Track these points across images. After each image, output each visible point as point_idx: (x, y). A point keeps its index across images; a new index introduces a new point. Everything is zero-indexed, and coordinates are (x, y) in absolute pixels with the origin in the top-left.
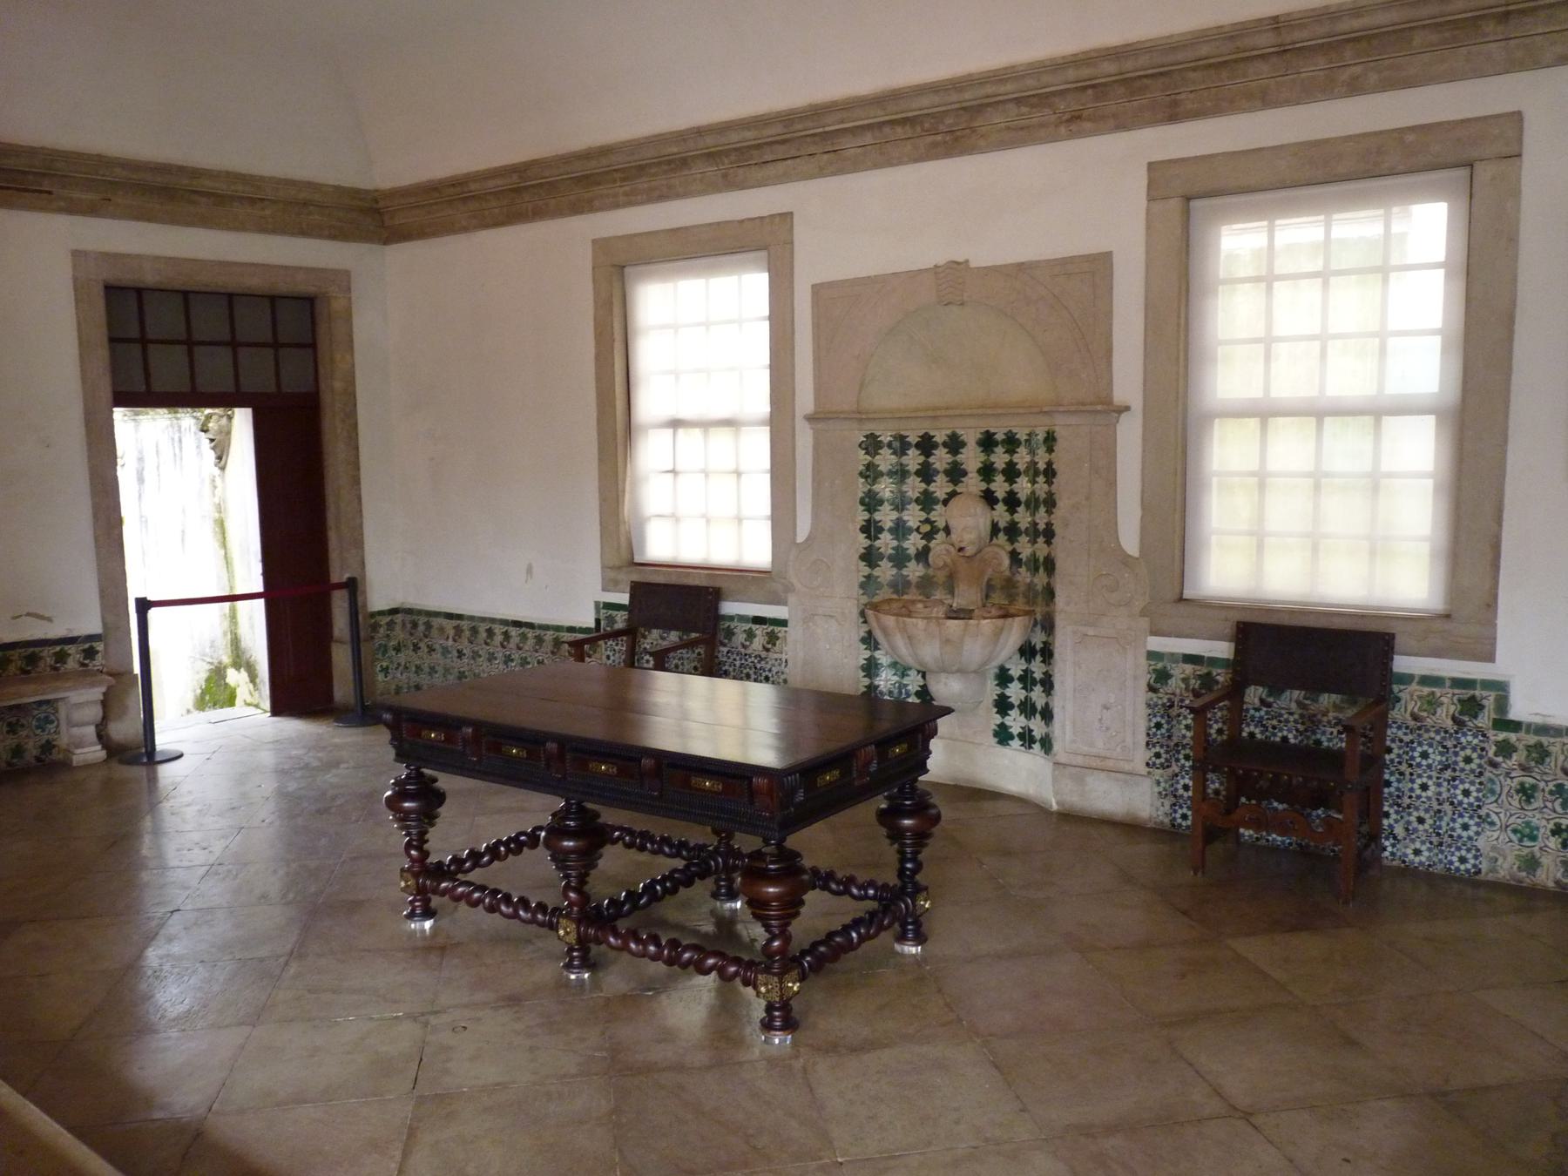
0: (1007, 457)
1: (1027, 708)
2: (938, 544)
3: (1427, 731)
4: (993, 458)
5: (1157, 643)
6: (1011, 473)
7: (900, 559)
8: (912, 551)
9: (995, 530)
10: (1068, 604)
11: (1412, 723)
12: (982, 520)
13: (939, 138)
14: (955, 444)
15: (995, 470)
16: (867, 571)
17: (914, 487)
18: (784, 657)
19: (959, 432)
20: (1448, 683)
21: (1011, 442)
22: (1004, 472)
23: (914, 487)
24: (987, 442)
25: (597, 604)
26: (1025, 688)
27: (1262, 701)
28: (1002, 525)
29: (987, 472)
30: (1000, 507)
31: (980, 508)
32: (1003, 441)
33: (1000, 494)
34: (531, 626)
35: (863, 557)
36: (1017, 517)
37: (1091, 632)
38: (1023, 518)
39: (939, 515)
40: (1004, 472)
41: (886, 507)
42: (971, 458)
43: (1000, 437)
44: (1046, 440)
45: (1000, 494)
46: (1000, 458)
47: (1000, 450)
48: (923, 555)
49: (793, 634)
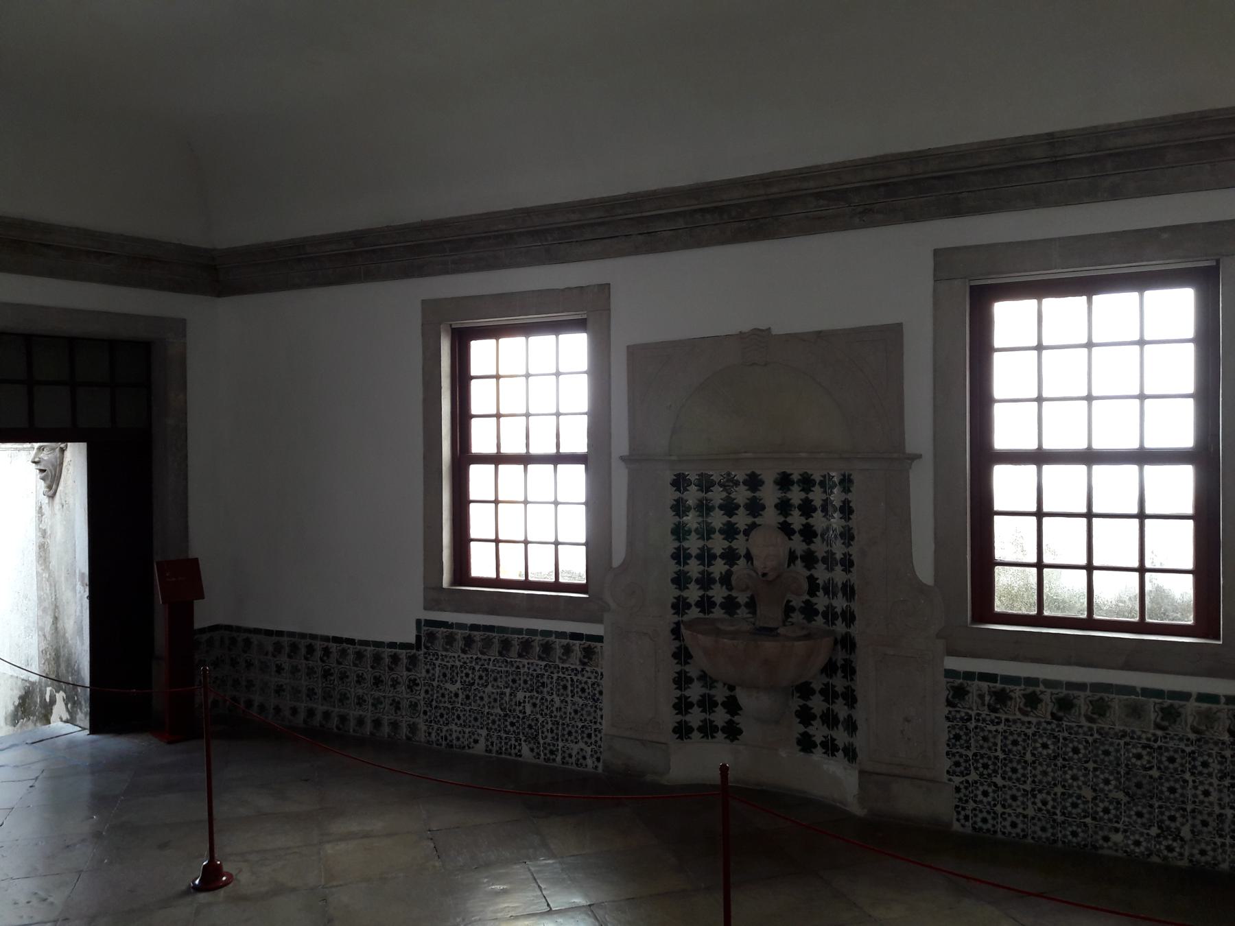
1: (830, 720)
3: (1207, 742)
4: (789, 495)
5: (952, 663)
6: (807, 508)
7: (706, 582)
8: (717, 576)
9: (792, 557)
11: (1193, 736)
13: (744, 224)
14: (754, 482)
16: (677, 593)
17: (718, 519)
18: (599, 670)
19: (758, 472)
20: (1223, 700)
21: (807, 483)
23: (718, 519)
24: (784, 481)
25: (418, 622)
26: (826, 700)
27: (1053, 715)
28: (799, 553)
29: (784, 507)
31: (780, 537)
32: (799, 481)
34: (351, 641)
35: (674, 581)
38: (819, 548)
39: (740, 544)
40: (800, 507)
41: (693, 536)
42: (769, 495)
43: (795, 477)
44: (842, 482)
46: (796, 496)
47: (796, 488)
48: (726, 580)
49: (606, 648)
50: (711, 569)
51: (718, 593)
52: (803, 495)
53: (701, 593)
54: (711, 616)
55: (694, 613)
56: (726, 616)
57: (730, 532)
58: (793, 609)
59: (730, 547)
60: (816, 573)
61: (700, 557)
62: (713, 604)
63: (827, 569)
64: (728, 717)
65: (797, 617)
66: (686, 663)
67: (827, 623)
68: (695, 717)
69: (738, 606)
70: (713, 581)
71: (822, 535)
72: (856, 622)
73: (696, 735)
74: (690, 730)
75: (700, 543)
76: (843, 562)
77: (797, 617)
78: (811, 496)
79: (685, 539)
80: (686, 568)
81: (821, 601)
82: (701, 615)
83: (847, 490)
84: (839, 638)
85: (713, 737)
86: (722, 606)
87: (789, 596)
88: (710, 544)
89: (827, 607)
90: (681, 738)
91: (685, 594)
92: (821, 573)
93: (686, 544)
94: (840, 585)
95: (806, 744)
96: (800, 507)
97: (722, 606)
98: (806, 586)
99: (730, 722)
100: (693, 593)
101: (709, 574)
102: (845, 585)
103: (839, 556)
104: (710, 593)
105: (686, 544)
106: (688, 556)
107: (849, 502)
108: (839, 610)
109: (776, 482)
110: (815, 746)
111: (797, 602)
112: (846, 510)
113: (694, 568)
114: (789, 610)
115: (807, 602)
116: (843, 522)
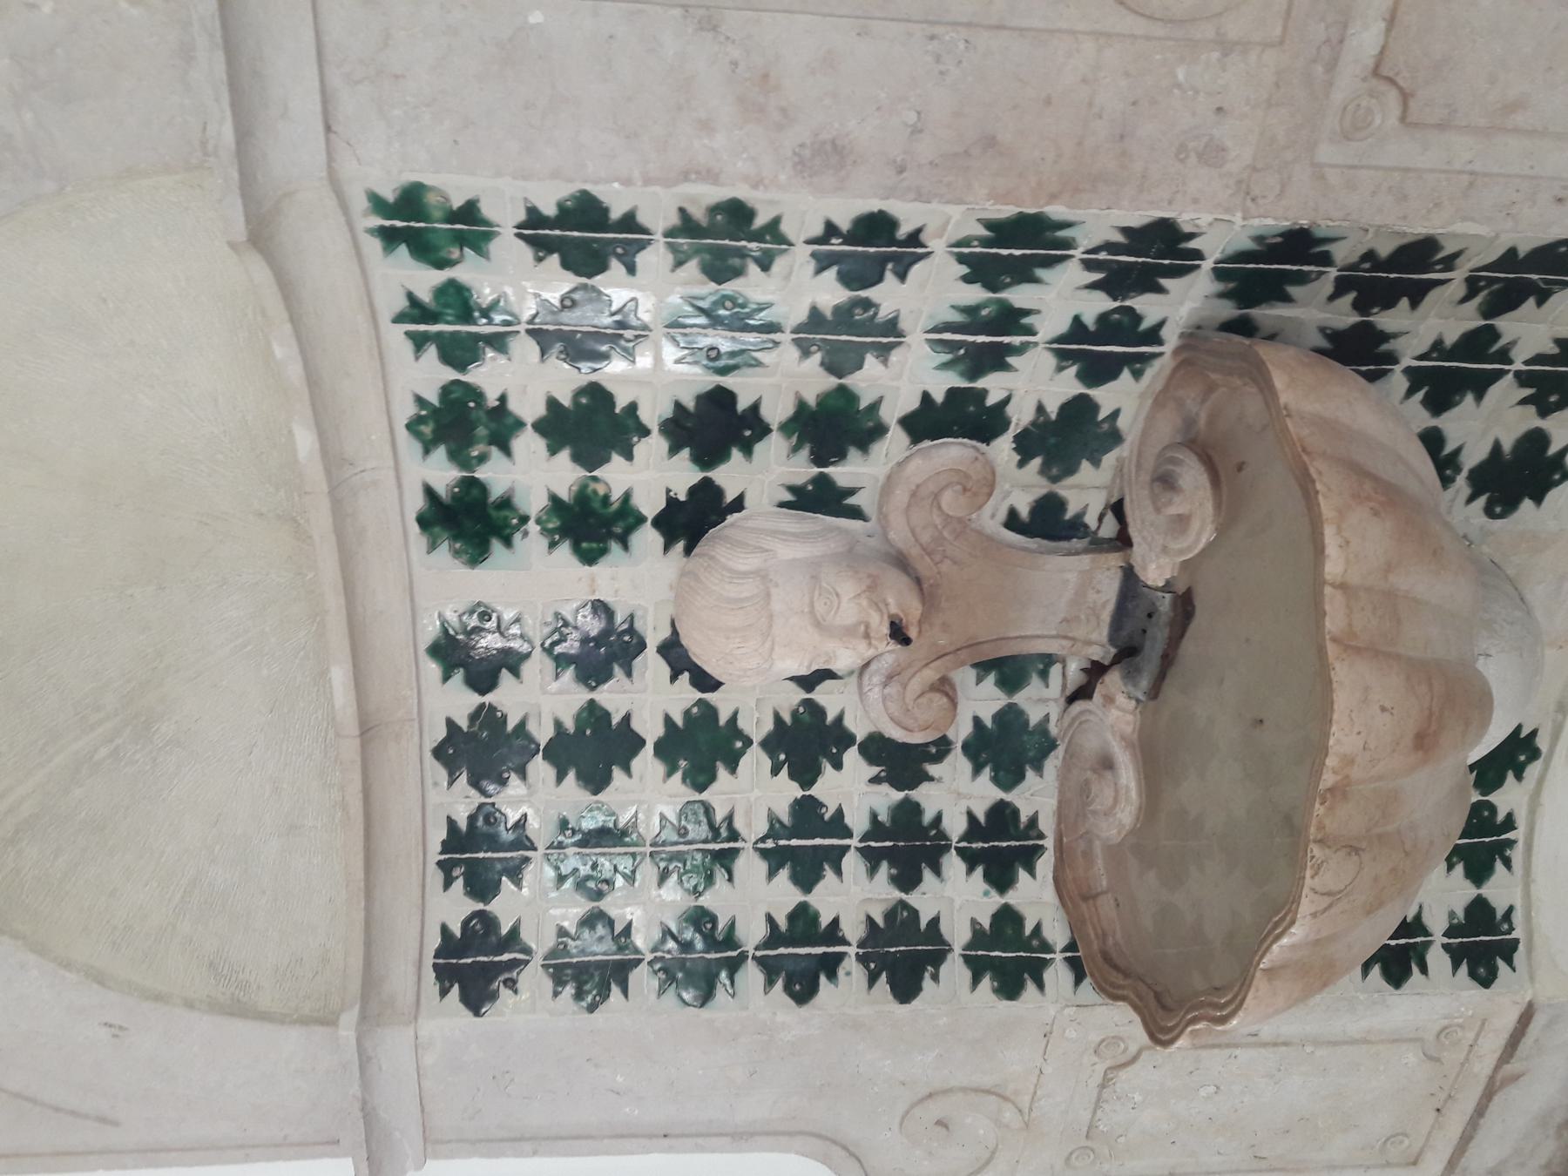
0: (528, 444)
2: (858, 709)
4: (534, 503)
6: (591, 426)
7: (908, 847)
8: (886, 798)
9: (820, 498)
12: (787, 552)
16: (954, 970)
17: (648, 795)
21: (458, 422)
23: (648, 795)
24: (469, 522)
26: (1480, 385)
28: (802, 470)
29: (589, 526)
30: (731, 476)
32: (458, 456)
33: (682, 475)
36: (776, 411)
38: (782, 381)
40: (590, 457)
43: (442, 474)
44: (425, 249)
45: (682, 475)
46: (532, 474)
47: (496, 474)
48: (901, 763)
50: (858, 822)
51: (956, 794)
53: (953, 864)
54: (1047, 825)
56: (1052, 764)
57: (701, 746)
59: (769, 745)
61: (808, 869)
62: (1002, 816)
63: (884, 352)
65: (1085, 493)
67: (1137, 365)
69: (1010, 718)
71: (724, 371)
72: (1186, 219)
73: (1500, 890)
74: (1480, 915)
75: (750, 866)
76: (860, 275)
77: (1085, 493)
79: (730, 941)
80: (853, 930)
81: (1033, 384)
82: (1045, 864)
83: (470, 228)
84: (1228, 310)
85: (1509, 824)
86: (1009, 776)
87: (991, 519)
88: (753, 827)
89: (1064, 357)
90: (1508, 950)
91: (958, 934)
92: (904, 378)
94: (975, 294)
96: (590, 457)
97: (1009, 776)
98: (953, 452)
100: (956, 898)
101: (877, 829)
102: (981, 270)
103: (829, 293)
104: (955, 826)
106: (803, 923)
107: (534, 219)
109: (476, 553)
111: (1022, 487)
112: (583, 235)
113: (853, 896)
114: (1048, 522)
115: (1026, 446)
116: (655, 258)
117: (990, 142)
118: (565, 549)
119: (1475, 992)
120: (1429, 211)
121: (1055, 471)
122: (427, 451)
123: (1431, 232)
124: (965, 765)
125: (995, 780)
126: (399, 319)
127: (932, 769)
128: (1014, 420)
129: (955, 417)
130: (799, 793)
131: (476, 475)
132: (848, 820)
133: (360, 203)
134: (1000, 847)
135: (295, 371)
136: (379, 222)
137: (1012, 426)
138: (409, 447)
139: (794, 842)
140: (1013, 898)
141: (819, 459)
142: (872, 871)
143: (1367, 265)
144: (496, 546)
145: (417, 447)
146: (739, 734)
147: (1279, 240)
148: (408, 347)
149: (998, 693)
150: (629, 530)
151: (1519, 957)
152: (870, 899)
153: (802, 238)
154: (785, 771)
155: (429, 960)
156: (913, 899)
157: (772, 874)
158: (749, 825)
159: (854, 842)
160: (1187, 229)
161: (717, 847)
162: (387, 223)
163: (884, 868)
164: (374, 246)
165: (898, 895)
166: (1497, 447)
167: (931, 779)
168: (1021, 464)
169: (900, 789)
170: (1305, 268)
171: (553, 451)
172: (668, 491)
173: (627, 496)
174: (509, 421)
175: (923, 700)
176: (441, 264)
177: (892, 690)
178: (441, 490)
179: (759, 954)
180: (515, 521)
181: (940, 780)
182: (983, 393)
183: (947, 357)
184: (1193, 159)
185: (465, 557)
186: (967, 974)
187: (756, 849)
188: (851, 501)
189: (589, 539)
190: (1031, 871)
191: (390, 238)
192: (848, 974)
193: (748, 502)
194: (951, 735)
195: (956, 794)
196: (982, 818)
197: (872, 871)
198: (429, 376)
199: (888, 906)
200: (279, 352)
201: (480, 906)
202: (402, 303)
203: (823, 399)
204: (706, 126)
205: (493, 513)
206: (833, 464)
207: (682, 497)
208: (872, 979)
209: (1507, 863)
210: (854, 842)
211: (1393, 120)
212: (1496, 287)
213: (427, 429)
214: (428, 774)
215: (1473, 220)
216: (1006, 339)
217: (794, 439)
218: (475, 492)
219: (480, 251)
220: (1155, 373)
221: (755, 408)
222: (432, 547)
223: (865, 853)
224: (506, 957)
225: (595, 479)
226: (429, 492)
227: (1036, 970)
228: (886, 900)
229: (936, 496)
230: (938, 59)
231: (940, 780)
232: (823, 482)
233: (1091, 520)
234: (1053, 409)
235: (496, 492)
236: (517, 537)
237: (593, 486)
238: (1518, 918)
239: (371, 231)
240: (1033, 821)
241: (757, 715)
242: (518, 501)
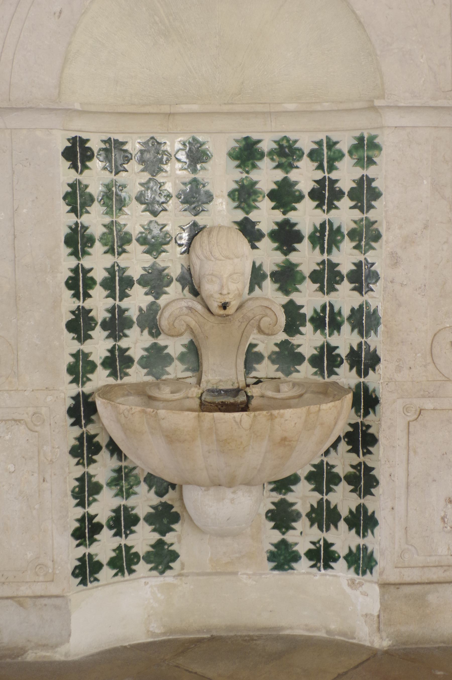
4: (254, 176)
9: (257, 276)
10: (399, 369)
15: (256, 193)
16: (75, 346)
22: (272, 195)
24: (247, 153)
28: (268, 269)
29: (244, 195)
30: (266, 244)
35: (71, 326)
37: (429, 404)
41: (98, 248)
43: (266, 145)
46: (266, 176)
50: (124, 304)
51: (136, 342)
52: (279, 175)
53: (110, 343)
54: (126, 380)
55: (100, 378)
56: (150, 378)
58: (259, 357)
60: (297, 298)
61: (108, 284)
62: (129, 361)
63: (321, 289)
64: (156, 536)
66: (91, 461)
68: (105, 546)
69: (168, 359)
70: (128, 323)
73: (106, 573)
74: (97, 567)
75: (109, 260)
78: (293, 176)
79: (85, 253)
80: (88, 304)
82: (111, 381)
86: (145, 363)
88: (123, 260)
91: (87, 347)
92: (309, 298)
93: (86, 262)
94: (346, 313)
95: (283, 557)
97: (145, 363)
98: (282, 319)
99: (160, 544)
100: (99, 346)
101: (122, 311)
104: (123, 343)
105: (86, 262)
108: (343, 352)
109: (233, 155)
110: (296, 558)
113: (99, 303)
114: (252, 358)
115: (284, 345)
117: (399, 305)
118: (235, 186)
119: (70, 569)
120: (386, 437)
121: (274, 356)
122: (275, 142)
123: (380, 440)
124: (147, 345)
125: (142, 357)
126: (328, 138)
127: (146, 332)
128: (294, 338)
129: (294, 318)
130: (135, 279)
131: (265, 157)
132: (125, 299)
133: (373, 133)
134: (117, 362)
135: (318, 108)
136: (366, 136)
137: (291, 338)
138: (278, 136)
139: (117, 278)
140: (100, 368)
141: (273, 275)
142: (108, 311)
143: (364, 428)
144: (237, 163)
145: (277, 139)
146: (159, 253)
147: (374, 396)
148: (317, 139)
149: (178, 353)
150: (243, 209)
151: (81, 586)
152: (98, 311)
153: (366, 257)
154: (144, 272)
155: (79, 134)
156: (98, 328)
157: (106, 269)
158: (123, 259)
159: (117, 302)
160: (377, 368)
161: (116, 247)
162: (366, 139)
163: (109, 315)
164: (358, 134)
165: (100, 321)
166: (293, 504)
167: (142, 332)
168: (276, 344)
169: (137, 319)
170: (362, 411)
171: (276, 183)
172: (259, 222)
173: (257, 208)
174: (288, 169)
175: (183, 323)
176: (350, 152)
177: (185, 311)
178: (259, 145)
179: (80, 265)
180: (247, 169)
181: (141, 335)
182: (305, 326)
183: (319, 310)
184: (397, 364)
185: (232, 152)
186: (74, 352)
187: (115, 262)
188: (257, 287)
189: (239, 194)
190: (109, 376)
191: (361, 139)
192: (74, 302)
193: (255, 250)
194: (161, 337)
195: (136, 342)
196: (127, 353)
197: (108, 311)
198: (306, 144)
199: (96, 318)
200: (326, 104)
201: (96, 154)
202: (334, 139)
203: (301, 273)
204: (401, 227)
205: (250, 162)
206: (272, 279)
207: (257, 227)
208: (73, 312)
209: (116, 575)
210: (117, 302)
211: (409, 419)
212: (358, 473)
213: (285, 143)
214: (144, 135)
215: (384, 451)
216: (327, 328)
217: (282, 265)
218: (259, 156)
219: (355, 165)
220: (319, 379)
221: (295, 250)
222: (237, 141)
223: (114, 308)
224: (79, 164)
225: (264, 197)
226: (259, 141)
227: (75, 381)
228: (98, 316)
229: (266, 315)
230: (420, 288)
231: (141, 335)
232: (264, 277)
233: (254, 374)
234: (299, 350)
235: (259, 163)
236: (241, 170)
237: (261, 196)
238: (95, 584)
239: (362, 134)
240: (127, 374)
241: (166, 260)
242: (255, 171)
